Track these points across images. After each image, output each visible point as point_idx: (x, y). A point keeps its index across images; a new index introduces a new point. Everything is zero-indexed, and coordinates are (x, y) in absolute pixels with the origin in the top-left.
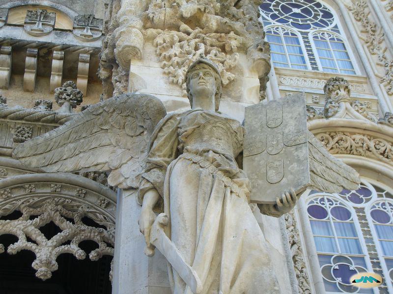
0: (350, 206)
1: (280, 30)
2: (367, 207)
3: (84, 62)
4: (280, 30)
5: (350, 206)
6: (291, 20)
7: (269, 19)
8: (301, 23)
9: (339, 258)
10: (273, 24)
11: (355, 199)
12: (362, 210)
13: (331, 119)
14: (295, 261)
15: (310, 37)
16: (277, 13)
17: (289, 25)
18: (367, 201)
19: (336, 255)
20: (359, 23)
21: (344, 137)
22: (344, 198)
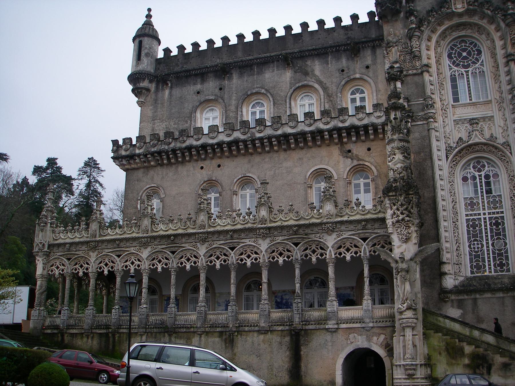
0: (477, 174)
1: (456, 72)
2: (483, 173)
3: (380, 129)
4: (456, 72)
5: (477, 174)
6: (461, 63)
7: (451, 65)
8: (466, 64)
9: (471, 198)
10: (453, 70)
11: (479, 171)
12: (480, 176)
13: (469, 143)
14: (453, 208)
15: (470, 73)
16: (455, 59)
17: (460, 67)
18: (484, 170)
19: (470, 197)
20: (492, 60)
21: (475, 147)
22: (475, 171)
